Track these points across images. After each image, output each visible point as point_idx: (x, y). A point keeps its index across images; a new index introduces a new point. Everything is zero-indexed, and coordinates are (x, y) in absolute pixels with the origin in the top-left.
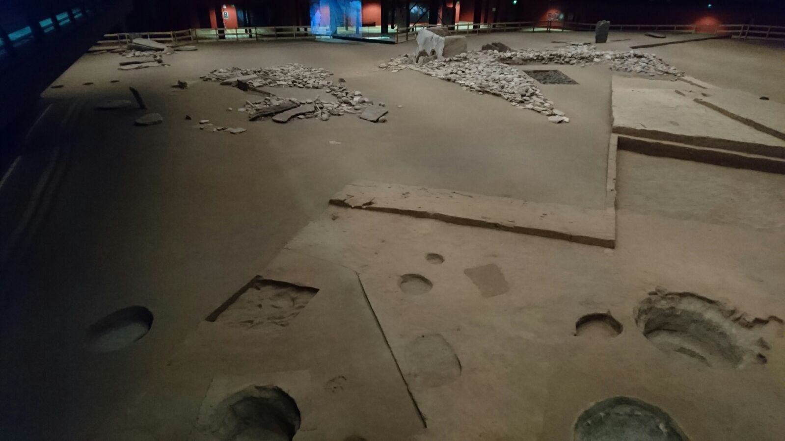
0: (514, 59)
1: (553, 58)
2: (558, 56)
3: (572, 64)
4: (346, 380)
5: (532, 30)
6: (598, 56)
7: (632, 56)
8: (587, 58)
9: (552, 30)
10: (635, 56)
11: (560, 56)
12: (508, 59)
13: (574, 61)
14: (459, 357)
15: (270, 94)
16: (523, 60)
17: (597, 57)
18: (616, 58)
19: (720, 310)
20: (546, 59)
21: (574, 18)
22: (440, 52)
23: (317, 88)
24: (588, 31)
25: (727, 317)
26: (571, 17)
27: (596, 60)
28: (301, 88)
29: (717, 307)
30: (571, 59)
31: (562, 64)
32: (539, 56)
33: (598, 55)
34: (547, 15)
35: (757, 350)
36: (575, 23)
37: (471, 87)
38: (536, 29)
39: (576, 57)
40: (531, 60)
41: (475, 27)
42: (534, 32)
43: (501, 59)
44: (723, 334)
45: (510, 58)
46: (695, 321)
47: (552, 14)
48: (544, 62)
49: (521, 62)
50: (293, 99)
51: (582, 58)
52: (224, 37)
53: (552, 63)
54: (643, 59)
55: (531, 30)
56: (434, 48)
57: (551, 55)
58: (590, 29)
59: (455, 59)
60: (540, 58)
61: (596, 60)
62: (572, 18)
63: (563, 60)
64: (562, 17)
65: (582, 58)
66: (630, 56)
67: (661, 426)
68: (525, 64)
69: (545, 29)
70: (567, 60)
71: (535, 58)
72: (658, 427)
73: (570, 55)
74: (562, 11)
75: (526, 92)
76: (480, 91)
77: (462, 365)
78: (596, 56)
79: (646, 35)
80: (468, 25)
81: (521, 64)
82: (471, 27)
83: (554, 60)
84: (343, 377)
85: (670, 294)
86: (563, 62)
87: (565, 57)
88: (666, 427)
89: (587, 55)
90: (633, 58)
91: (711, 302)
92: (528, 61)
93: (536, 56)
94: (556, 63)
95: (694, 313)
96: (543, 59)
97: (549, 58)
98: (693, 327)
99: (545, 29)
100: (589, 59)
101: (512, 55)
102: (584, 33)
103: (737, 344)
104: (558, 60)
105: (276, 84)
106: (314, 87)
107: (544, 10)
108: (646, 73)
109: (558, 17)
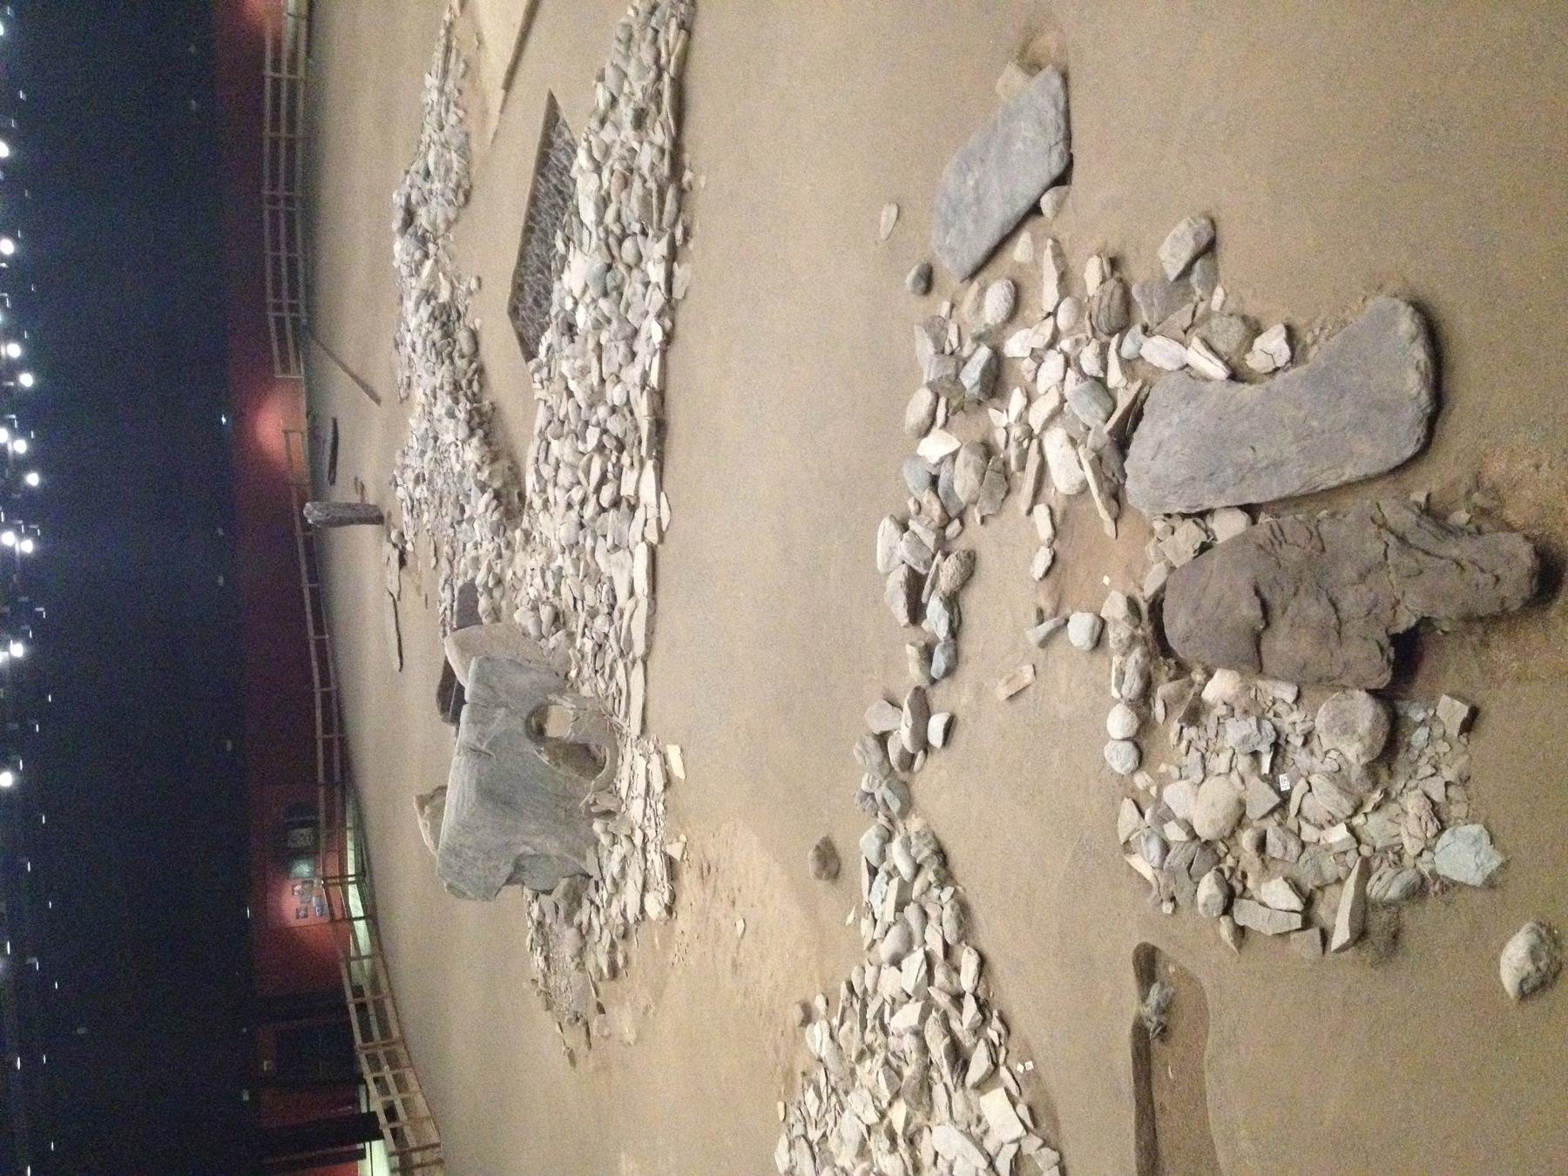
0: (497, 484)
5: (361, 927)
9: (351, 870)
12: (505, 501)
13: (462, 337)
15: (1140, 1032)
21: (302, 825)
23: (941, 853)
26: (302, 836)
27: (444, 296)
28: (983, 962)
31: (480, 371)
34: (303, 922)
36: (322, 817)
37: (673, 256)
38: (356, 907)
47: (298, 904)
49: (504, 463)
50: (1119, 722)
54: (414, 199)
55: (361, 927)
56: (518, 725)
60: (477, 419)
61: (444, 296)
64: (303, 869)
69: (353, 891)
76: (681, 192)
79: (333, 482)
99: (353, 891)
100: (446, 318)
102: (349, 715)
105: (1032, 1145)
106: (946, 875)
107: (286, 939)
108: (460, 91)
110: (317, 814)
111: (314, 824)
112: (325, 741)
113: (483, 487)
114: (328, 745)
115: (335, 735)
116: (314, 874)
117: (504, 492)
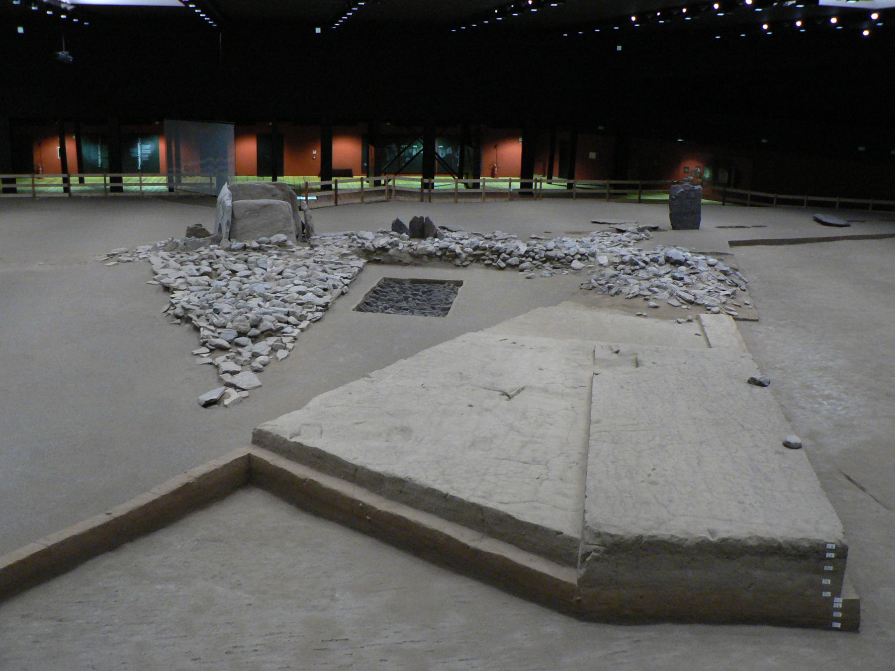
0: (391, 252)
1: (484, 255)
2: (493, 253)
3: (522, 270)
6: (583, 257)
7: (662, 260)
8: (559, 259)
10: (668, 260)
11: (498, 252)
16: (411, 255)
17: (579, 260)
18: (623, 263)
20: (464, 255)
22: (225, 230)
24: (746, 205)
26: (724, 176)
27: (576, 264)
30: (524, 259)
32: (447, 248)
33: (582, 255)
34: (682, 171)
39: (537, 257)
40: (431, 255)
41: (523, 185)
42: (640, 201)
43: (365, 250)
45: (383, 249)
47: (691, 169)
48: (458, 262)
49: (408, 259)
51: (549, 259)
52: (120, 189)
53: (478, 265)
57: (477, 248)
58: (748, 202)
59: (255, 244)
61: (576, 264)
62: (726, 179)
63: (504, 260)
64: (707, 175)
65: (549, 259)
66: (655, 260)
68: (416, 265)
70: (513, 260)
71: (439, 254)
73: (523, 249)
74: (707, 164)
75: (252, 326)
78: (579, 256)
80: (510, 181)
81: (406, 264)
82: (517, 185)
83: (484, 260)
86: (503, 265)
87: (510, 254)
89: (560, 254)
90: (661, 265)
92: (425, 258)
93: (441, 249)
94: (488, 265)
96: (457, 256)
97: (470, 255)
101: (391, 244)
104: (492, 260)
109: (701, 174)
110: (735, 187)
111: (728, 185)
112: (746, 195)
113: (394, 245)
114: (743, 197)
115: (748, 202)
116: (704, 180)
117: (385, 254)
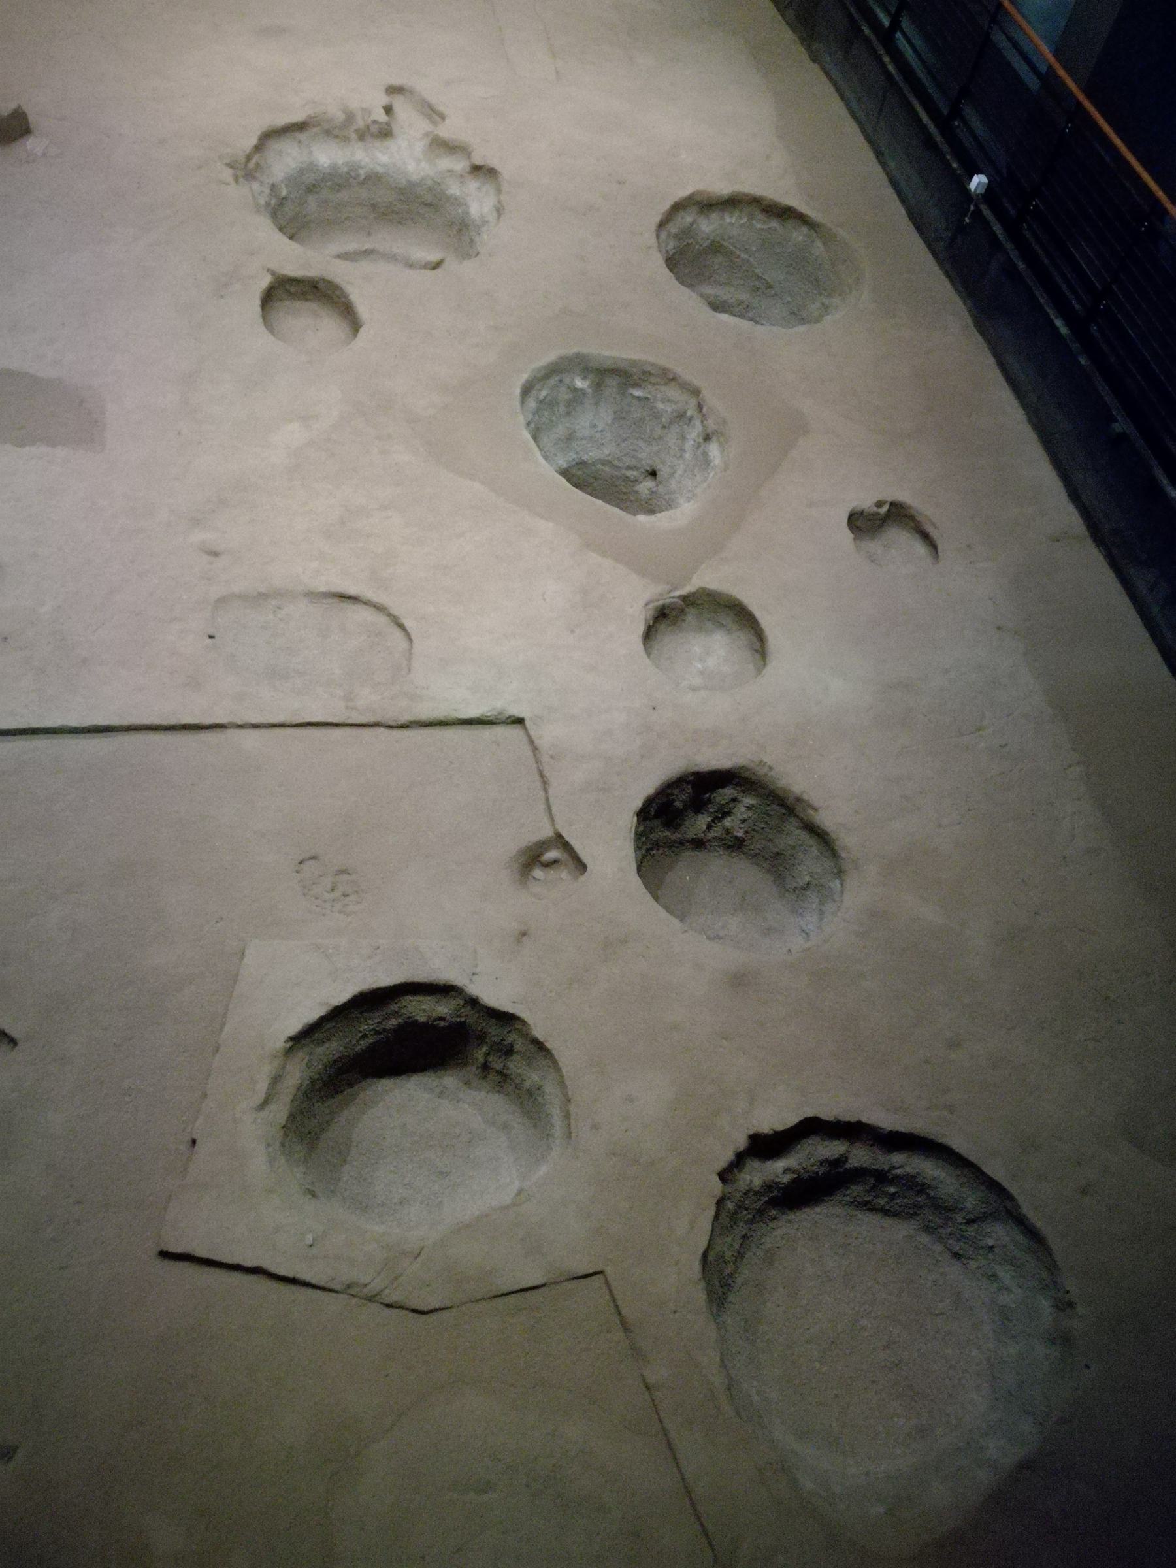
4: (314, 858)
14: (323, 589)
19: (328, 132)
25: (346, 139)
29: (316, 130)
35: (459, 165)
44: (373, 179)
46: (311, 189)
67: (579, 383)
72: (576, 390)
77: (352, 591)
84: (301, 863)
85: (249, 158)
88: (584, 378)
91: (301, 127)
95: (301, 172)
98: (312, 203)
103: (414, 178)
